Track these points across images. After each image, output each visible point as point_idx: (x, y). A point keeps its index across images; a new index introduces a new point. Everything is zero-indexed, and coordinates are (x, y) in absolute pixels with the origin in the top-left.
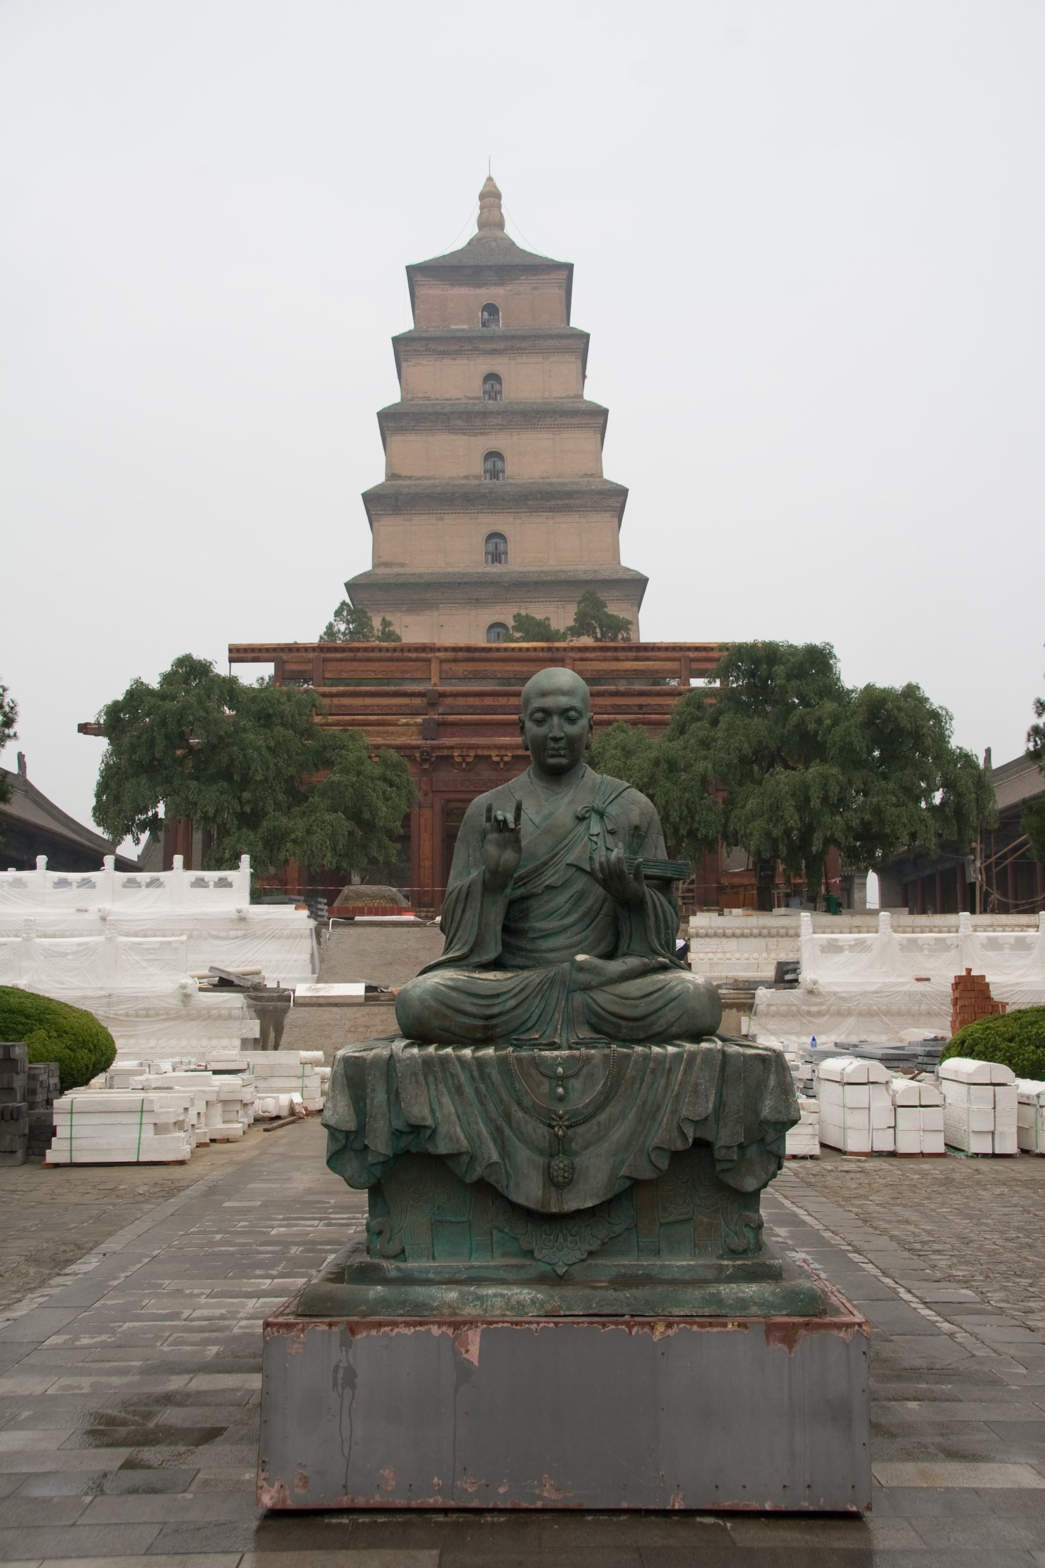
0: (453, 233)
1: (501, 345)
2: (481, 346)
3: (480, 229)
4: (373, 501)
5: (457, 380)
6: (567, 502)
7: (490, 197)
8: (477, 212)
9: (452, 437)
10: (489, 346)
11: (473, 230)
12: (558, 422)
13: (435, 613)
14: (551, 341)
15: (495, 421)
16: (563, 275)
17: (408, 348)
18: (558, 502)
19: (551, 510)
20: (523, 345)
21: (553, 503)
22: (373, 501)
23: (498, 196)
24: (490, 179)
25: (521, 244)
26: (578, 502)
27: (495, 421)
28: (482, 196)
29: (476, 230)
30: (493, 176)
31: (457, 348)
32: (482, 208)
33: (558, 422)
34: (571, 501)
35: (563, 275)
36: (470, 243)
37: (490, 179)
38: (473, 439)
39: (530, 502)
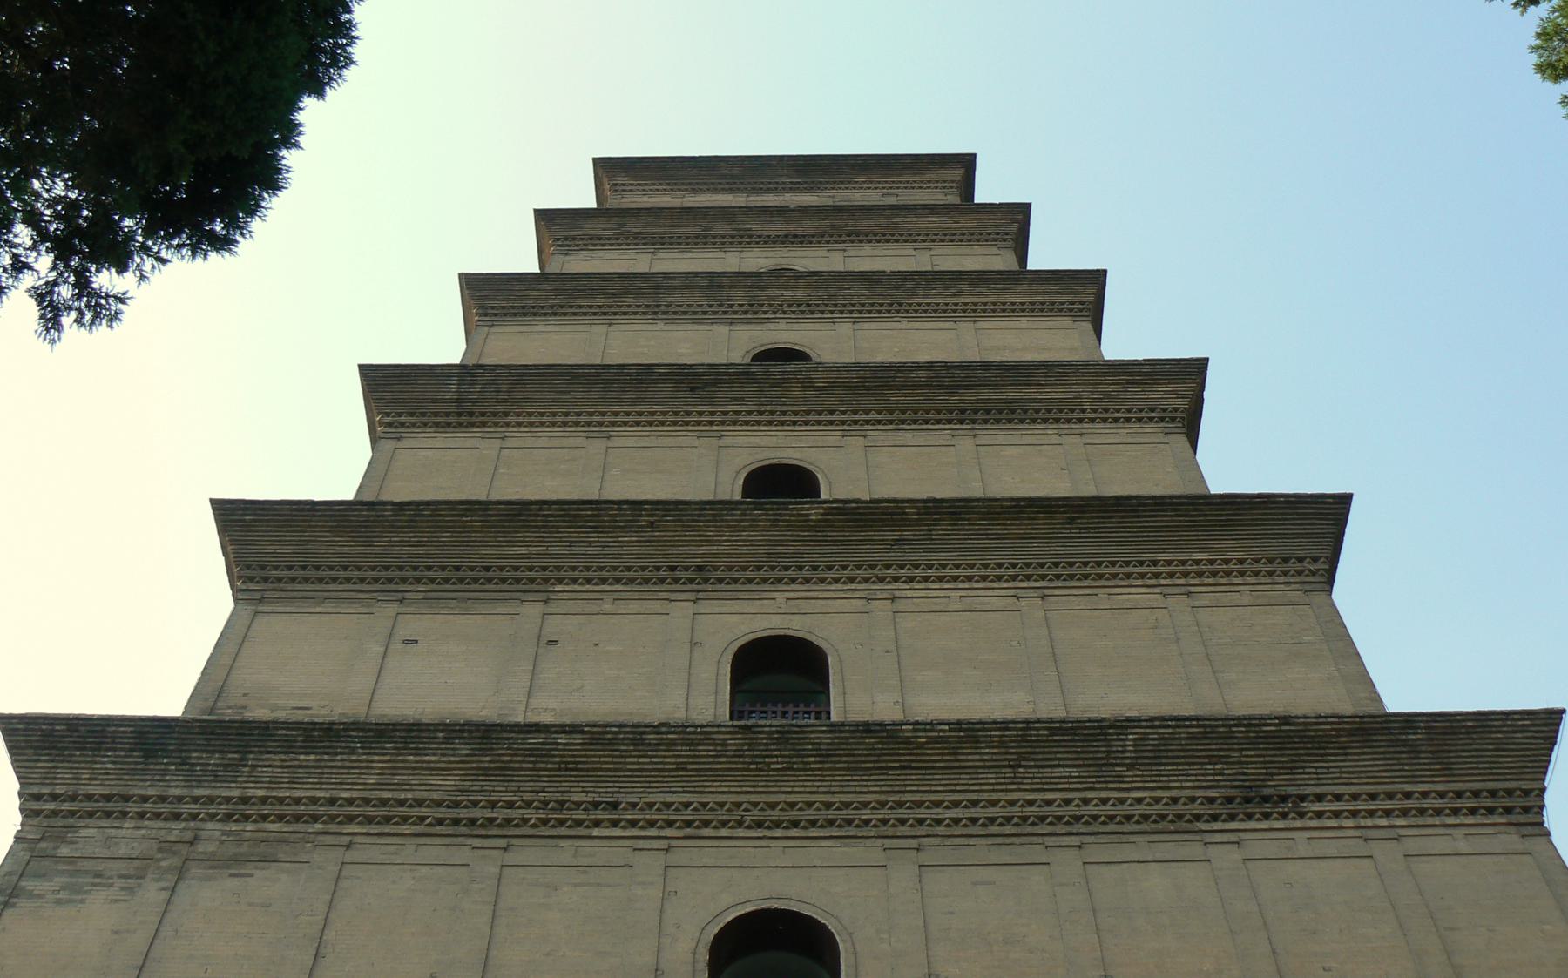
1: (808, 226)
2: (756, 227)
6: (1011, 393)
9: (661, 325)
10: (777, 228)
12: (969, 299)
13: (532, 611)
14: (935, 220)
15: (788, 296)
16: (956, 174)
17: (573, 233)
18: (985, 393)
19: (966, 417)
20: (865, 224)
21: (969, 395)
26: (1050, 394)
27: (788, 296)
31: (698, 230)
33: (962, 299)
34: (1028, 392)
35: (956, 174)
38: (724, 329)
39: (894, 396)
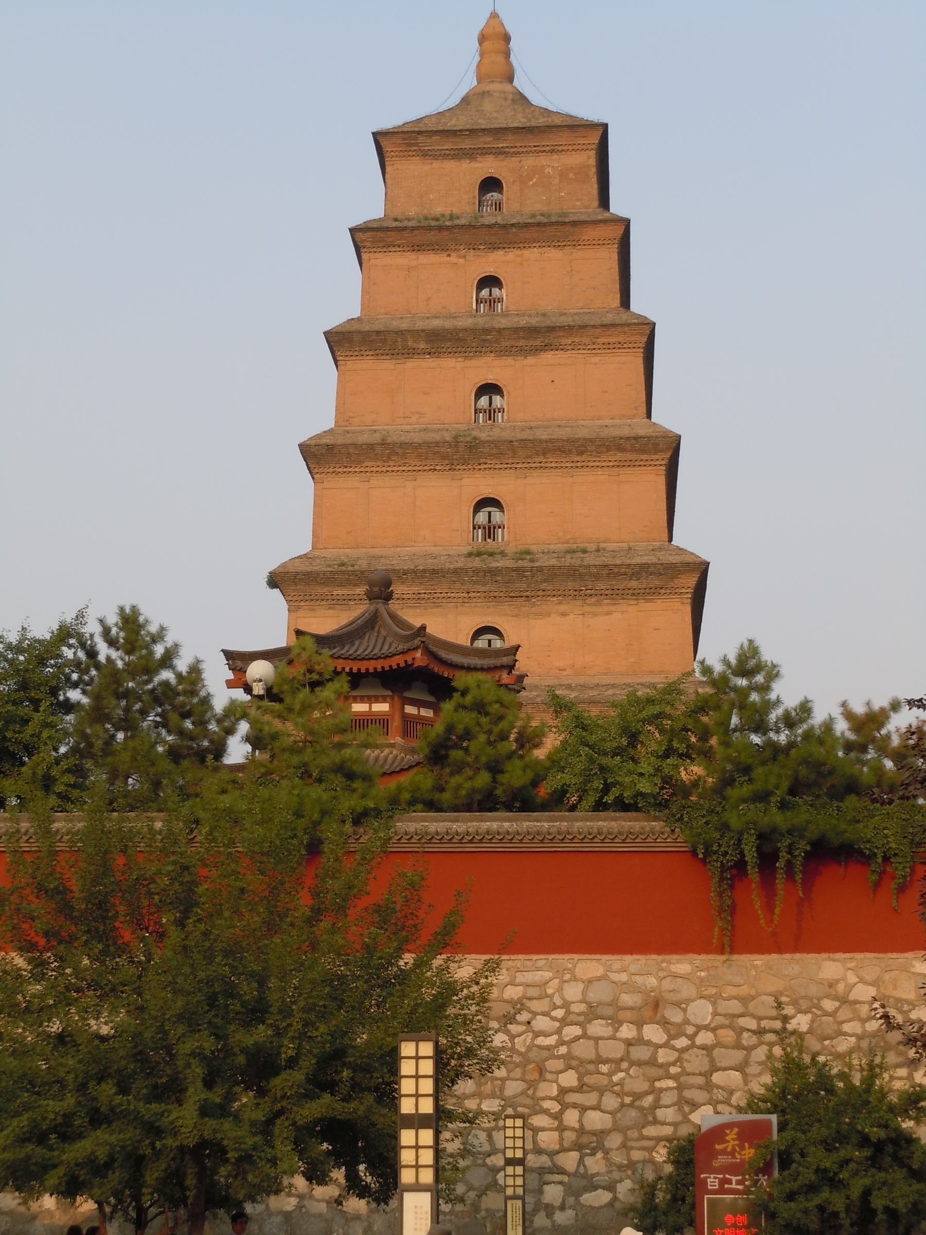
0: (440, 84)
3: (480, 80)
4: (317, 455)
5: (441, 286)
7: (496, 41)
8: (477, 58)
11: (469, 82)
22: (317, 455)
23: (507, 38)
24: (494, 16)
25: (536, 99)
28: (482, 39)
29: (475, 83)
30: (498, 10)
32: (482, 55)
36: (466, 101)
37: (494, 16)
